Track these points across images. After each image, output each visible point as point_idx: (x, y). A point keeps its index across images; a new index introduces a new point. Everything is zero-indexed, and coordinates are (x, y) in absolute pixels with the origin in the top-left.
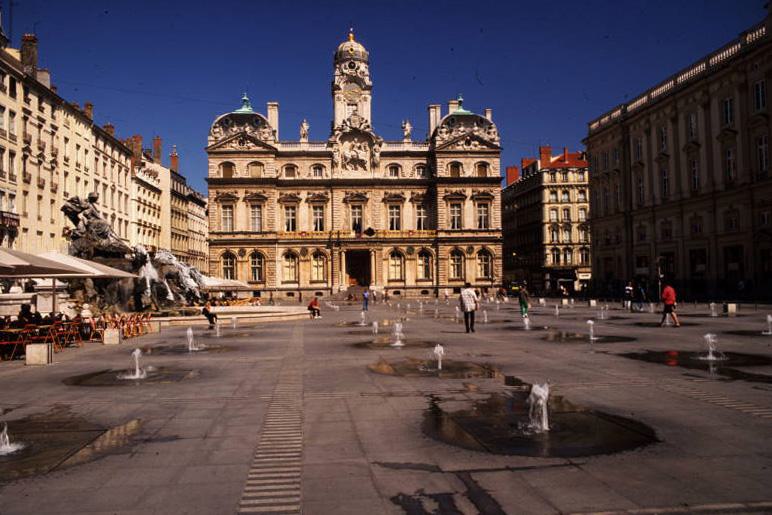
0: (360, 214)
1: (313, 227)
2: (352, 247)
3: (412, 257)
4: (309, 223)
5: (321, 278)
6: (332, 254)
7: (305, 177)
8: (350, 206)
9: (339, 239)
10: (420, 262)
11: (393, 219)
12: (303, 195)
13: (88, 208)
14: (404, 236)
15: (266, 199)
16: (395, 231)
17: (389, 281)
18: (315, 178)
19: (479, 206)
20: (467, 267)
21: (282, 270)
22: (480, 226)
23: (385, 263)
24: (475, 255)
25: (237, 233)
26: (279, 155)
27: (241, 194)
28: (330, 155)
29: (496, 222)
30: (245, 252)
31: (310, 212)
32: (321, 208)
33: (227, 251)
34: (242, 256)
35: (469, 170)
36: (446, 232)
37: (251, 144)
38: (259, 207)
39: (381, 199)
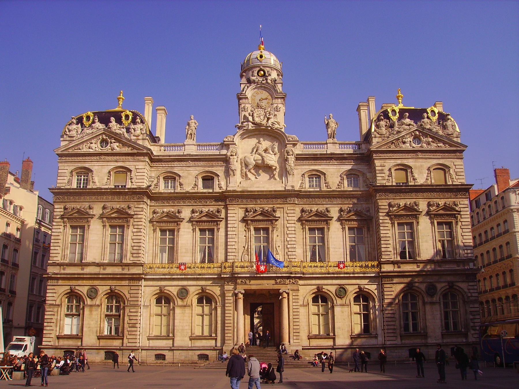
0: (267, 240)
1: (199, 257)
2: (255, 285)
4: (193, 253)
5: (206, 333)
6: (223, 295)
7: (188, 188)
10: (356, 308)
11: (314, 246)
14: (331, 270)
15: (131, 216)
16: (319, 264)
18: (205, 191)
20: (429, 317)
23: (303, 311)
26: (154, 160)
27: (97, 210)
28: (226, 160)
30: (96, 291)
31: (194, 238)
32: (212, 231)
36: (393, 263)
37: (115, 145)
38: (122, 227)
39: (296, 219)
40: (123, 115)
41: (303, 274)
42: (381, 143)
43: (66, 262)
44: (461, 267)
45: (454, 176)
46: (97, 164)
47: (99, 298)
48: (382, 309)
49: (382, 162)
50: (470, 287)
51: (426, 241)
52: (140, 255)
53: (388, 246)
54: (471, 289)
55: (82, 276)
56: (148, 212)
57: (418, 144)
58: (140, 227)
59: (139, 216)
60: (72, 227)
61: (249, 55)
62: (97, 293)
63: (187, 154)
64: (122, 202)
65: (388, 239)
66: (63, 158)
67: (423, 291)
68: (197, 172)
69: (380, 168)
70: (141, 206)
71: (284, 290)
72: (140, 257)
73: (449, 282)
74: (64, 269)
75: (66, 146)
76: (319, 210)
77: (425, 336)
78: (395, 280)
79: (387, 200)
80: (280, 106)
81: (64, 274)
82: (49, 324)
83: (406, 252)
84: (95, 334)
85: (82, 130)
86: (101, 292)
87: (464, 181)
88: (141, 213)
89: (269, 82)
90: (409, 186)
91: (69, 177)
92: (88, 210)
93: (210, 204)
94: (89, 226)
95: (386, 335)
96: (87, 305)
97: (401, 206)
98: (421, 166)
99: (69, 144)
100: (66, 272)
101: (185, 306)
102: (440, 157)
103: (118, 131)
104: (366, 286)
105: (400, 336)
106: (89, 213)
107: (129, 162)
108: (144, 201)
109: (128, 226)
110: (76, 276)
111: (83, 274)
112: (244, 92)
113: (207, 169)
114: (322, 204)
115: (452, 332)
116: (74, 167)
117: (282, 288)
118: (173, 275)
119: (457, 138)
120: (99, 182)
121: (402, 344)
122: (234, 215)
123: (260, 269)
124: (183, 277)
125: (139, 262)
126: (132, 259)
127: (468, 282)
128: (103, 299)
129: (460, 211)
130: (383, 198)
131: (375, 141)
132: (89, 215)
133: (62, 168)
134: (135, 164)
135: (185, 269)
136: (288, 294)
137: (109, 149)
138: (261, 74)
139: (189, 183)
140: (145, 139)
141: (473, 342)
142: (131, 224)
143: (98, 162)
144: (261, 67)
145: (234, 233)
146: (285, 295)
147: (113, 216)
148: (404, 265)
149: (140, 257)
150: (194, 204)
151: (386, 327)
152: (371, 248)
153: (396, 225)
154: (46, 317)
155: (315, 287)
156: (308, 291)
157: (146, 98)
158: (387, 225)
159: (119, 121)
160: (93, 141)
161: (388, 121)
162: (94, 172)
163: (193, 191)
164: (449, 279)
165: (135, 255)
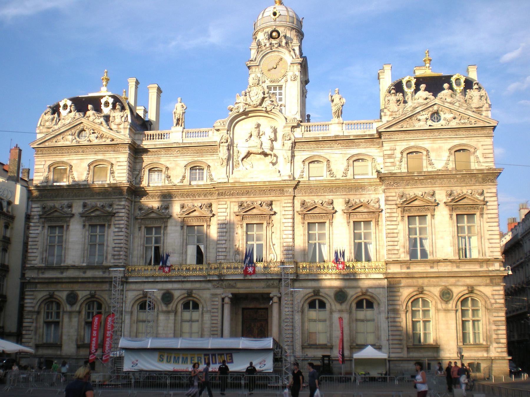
2: (242, 289)
3: (344, 306)
8: (245, 225)
9: (220, 275)
17: (303, 347)
20: (442, 326)
21: (131, 327)
25: (68, 268)
33: (51, 296)
34: (72, 303)
40: (103, 101)
41: (297, 275)
42: (391, 123)
43: (43, 265)
44: (485, 268)
45: (481, 159)
46: (76, 158)
47: (79, 304)
48: (387, 316)
49: (392, 144)
50: (495, 293)
51: (442, 238)
52: (121, 257)
53: (396, 243)
54: (496, 295)
55: (60, 281)
56: (131, 209)
57: (437, 122)
58: (122, 226)
59: (121, 214)
60: (51, 227)
61: (262, 12)
62: (77, 299)
63: (174, 143)
64: (102, 199)
65: (395, 235)
66: (39, 153)
67: (435, 296)
69: (389, 152)
70: (123, 203)
71: (275, 294)
72: (121, 259)
73: (468, 286)
74: (43, 273)
75: (42, 138)
76: (321, 202)
79: (396, 190)
81: (42, 278)
82: (28, 332)
83: (416, 250)
84: (74, 343)
85: (59, 120)
86: (80, 297)
87: (492, 165)
88: (123, 211)
89: (283, 44)
90: (421, 172)
91: (46, 173)
92: (65, 210)
93: (199, 198)
94: (68, 226)
95: (391, 346)
96: (66, 312)
97: (412, 197)
98: (440, 148)
99: (45, 137)
100: (44, 276)
101: (168, 312)
102: (464, 136)
103: (97, 121)
104: (370, 290)
105: (408, 348)
106: (68, 212)
107: (109, 154)
108: (125, 198)
109: (109, 226)
110: (55, 281)
111: (61, 278)
112: (254, 59)
113: (196, 159)
114: (324, 195)
115: (471, 345)
117: (274, 293)
118: (157, 277)
119: (487, 112)
120: (77, 178)
121: (408, 357)
122: (224, 210)
123: (248, 271)
124: (167, 280)
125: (120, 264)
126: (112, 261)
127: (493, 286)
128: (84, 305)
129: (487, 202)
130: (390, 187)
131: (385, 119)
132: (68, 214)
133: (39, 163)
134: (116, 156)
135: (169, 271)
136: (280, 299)
137: (88, 141)
138: (276, 35)
139: (176, 176)
140: (126, 128)
141: (495, 357)
142: (112, 223)
143: (77, 156)
144: (274, 27)
145: (225, 230)
146: (275, 299)
147: (93, 214)
148: (414, 265)
149: (121, 259)
150: (182, 199)
151: (391, 337)
152: (379, 245)
153: (406, 219)
154: (25, 324)
155: (310, 290)
156: (302, 295)
157: (130, 79)
158: (395, 219)
159: (98, 109)
160: (70, 132)
161: (401, 94)
163: (181, 184)
164: (469, 281)
165: (116, 257)
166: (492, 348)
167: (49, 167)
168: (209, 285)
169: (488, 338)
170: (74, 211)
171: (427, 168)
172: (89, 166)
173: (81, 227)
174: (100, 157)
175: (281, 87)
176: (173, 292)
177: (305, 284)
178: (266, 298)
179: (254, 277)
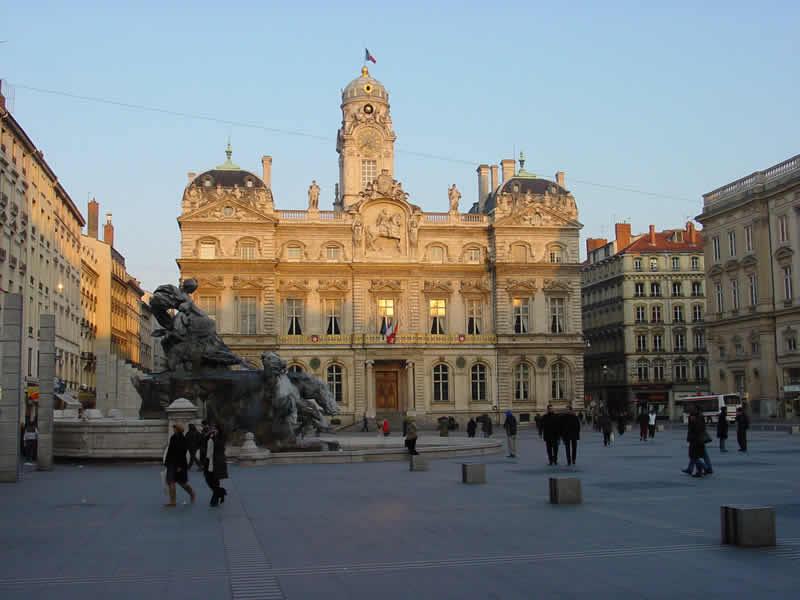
7: (314, 259)
12: (313, 284)
13: (183, 301)
14: (453, 342)
15: (261, 289)
19: (553, 300)
22: (554, 328)
24: (547, 368)
29: (574, 322)
35: (540, 255)
49: (503, 238)
68: (321, 242)
69: (500, 245)
77: (535, 402)
78: (511, 352)
80: (390, 151)
91: (194, 247)
94: (220, 298)
109: (260, 299)
116: (199, 237)
136: (413, 364)
155: (437, 357)
162: (221, 242)
166: (573, 402)
167: (197, 241)
168: (352, 353)
169: (572, 394)
170: (225, 284)
171: (530, 261)
172: (237, 242)
173: (233, 299)
174: (247, 234)
175: (374, 162)
176: (321, 359)
177: (432, 352)
178: (403, 364)
179: (393, 347)
